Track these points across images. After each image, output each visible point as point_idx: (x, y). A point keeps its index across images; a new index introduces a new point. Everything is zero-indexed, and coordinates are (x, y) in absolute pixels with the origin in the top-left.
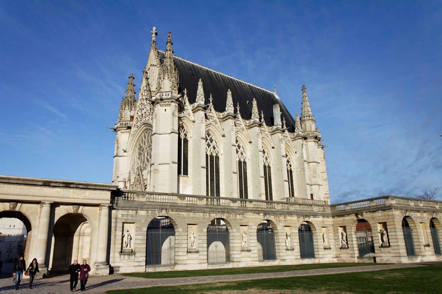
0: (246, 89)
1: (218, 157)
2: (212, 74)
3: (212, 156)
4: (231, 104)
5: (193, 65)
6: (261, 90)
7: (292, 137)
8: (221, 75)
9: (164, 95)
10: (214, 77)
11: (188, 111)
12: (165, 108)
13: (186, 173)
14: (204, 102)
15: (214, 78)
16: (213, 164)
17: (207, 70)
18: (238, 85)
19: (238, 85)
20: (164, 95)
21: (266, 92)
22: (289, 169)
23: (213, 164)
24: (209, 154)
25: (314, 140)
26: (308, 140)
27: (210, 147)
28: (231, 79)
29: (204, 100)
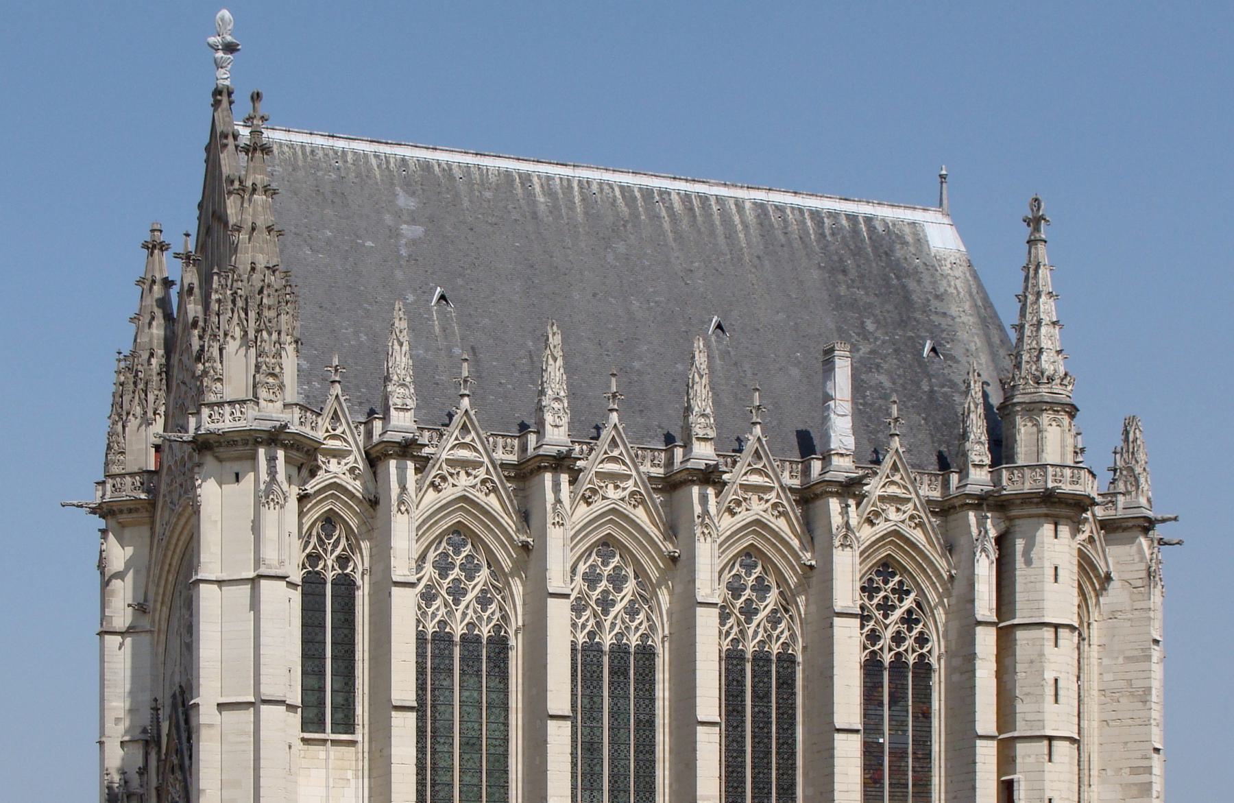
0: (730, 235)
1: (504, 640)
2: (530, 195)
3: (470, 641)
4: (557, 399)
5: (426, 166)
6: (834, 215)
7: (936, 494)
8: (585, 185)
9: (227, 417)
10: (542, 207)
11: (351, 458)
12: (236, 467)
13: (346, 723)
14: (409, 415)
15: (535, 215)
16: (469, 672)
17: (508, 174)
18: (685, 224)
19: (685, 224)
20: (227, 417)
21: (869, 220)
22: (912, 659)
23: (469, 672)
24: (458, 630)
25: (1044, 510)
26: (1014, 513)
27: (462, 606)
28: (647, 193)
29: (411, 404)
